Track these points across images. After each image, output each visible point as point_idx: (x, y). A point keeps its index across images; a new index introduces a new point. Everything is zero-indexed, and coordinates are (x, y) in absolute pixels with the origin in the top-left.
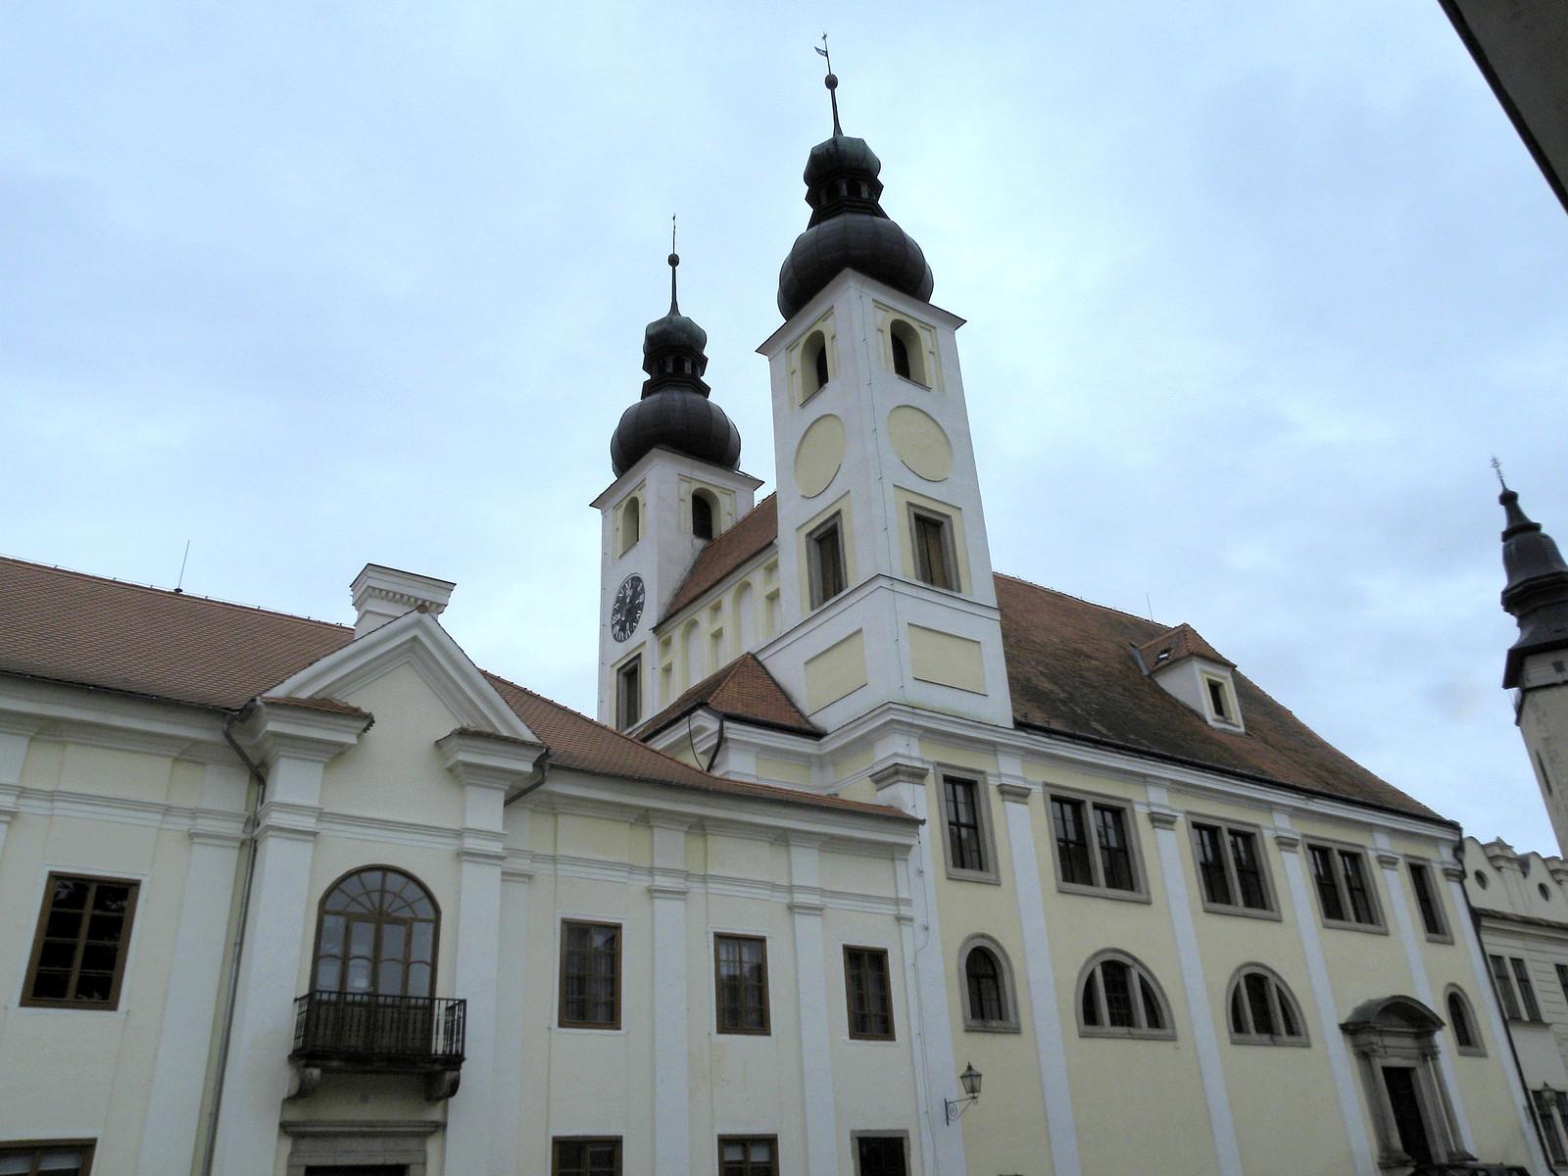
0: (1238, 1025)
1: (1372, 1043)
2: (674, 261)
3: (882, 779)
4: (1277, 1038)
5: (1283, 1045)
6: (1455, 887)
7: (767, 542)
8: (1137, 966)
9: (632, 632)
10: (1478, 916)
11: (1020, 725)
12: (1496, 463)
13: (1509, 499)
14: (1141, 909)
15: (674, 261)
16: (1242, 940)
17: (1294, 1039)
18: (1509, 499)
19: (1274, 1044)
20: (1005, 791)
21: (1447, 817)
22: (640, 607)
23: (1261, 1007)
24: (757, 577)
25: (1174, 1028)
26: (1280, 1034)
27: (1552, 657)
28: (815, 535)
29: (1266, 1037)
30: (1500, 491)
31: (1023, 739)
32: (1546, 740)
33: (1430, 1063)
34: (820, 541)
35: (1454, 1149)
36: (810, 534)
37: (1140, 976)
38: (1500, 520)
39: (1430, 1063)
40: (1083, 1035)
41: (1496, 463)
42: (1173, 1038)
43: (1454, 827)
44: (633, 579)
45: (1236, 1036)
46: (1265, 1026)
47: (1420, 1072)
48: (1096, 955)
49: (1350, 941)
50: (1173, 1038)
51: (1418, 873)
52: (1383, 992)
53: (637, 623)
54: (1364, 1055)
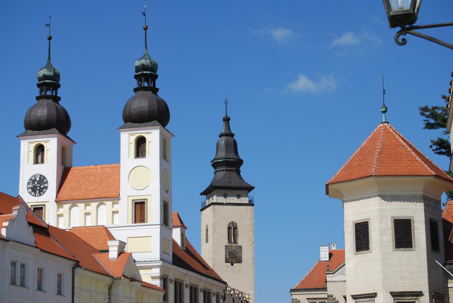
3: (153, 278)
6: (222, 300)
7: (114, 194)
9: (40, 195)
11: (174, 264)
12: (226, 102)
13: (227, 120)
15: (50, 39)
18: (227, 120)
20: (170, 280)
21: (224, 280)
22: (46, 188)
24: (109, 204)
28: (136, 201)
30: (224, 115)
32: (214, 224)
34: (136, 203)
36: (133, 200)
41: (226, 102)
43: (225, 283)
44: (41, 175)
51: (218, 296)
53: (44, 193)
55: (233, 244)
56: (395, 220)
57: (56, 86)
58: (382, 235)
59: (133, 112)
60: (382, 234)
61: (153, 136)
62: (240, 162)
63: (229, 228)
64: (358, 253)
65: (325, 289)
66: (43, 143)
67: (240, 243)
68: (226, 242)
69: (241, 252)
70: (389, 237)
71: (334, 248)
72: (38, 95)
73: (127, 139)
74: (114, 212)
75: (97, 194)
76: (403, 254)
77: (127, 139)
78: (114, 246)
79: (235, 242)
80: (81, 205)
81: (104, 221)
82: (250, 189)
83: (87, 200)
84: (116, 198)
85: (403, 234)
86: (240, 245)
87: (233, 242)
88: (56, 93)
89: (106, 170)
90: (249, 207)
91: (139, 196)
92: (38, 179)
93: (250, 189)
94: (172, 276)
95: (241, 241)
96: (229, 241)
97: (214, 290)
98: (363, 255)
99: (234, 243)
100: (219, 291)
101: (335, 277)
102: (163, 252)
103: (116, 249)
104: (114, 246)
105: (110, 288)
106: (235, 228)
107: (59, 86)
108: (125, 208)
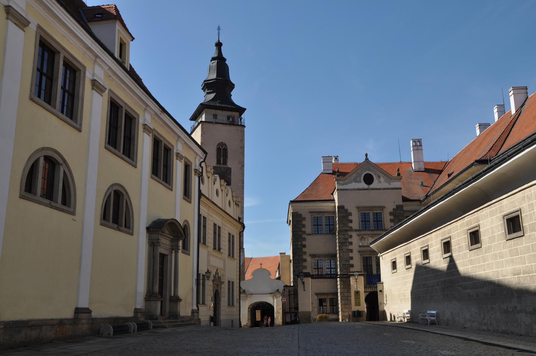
0: (105, 216)
1: (159, 239)
4: (120, 228)
5: (122, 231)
8: (64, 165)
10: (200, 194)
12: (219, 29)
13: (219, 45)
14: (76, 132)
16: (118, 170)
17: (127, 230)
18: (219, 45)
19: (119, 230)
23: (116, 210)
25: (75, 208)
26: (122, 226)
27: (214, 111)
29: (116, 226)
30: (217, 41)
33: (173, 255)
35: (172, 295)
37: (64, 172)
38: (213, 53)
39: (173, 255)
40: (22, 197)
41: (219, 29)
42: (73, 213)
45: (103, 222)
46: (116, 220)
47: (169, 256)
48: (43, 149)
49: (160, 188)
50: (73, 213)
51: (187, 167)
52: (166, 216)
54: (153, 244)
55: (222, 166)
62: (232, 86)
63: (218, 150)
67: (229, 164)
69: (230, 174)
79: (225, 163)
82: (241, 110)
86: (229, 166)
87: (222, 162)
90: (240, 128)
93: (241, 110)
96: (218, 162)
99: (223, 164)
100: (191, 157)
101: (347, 184)
106: (225, 150)
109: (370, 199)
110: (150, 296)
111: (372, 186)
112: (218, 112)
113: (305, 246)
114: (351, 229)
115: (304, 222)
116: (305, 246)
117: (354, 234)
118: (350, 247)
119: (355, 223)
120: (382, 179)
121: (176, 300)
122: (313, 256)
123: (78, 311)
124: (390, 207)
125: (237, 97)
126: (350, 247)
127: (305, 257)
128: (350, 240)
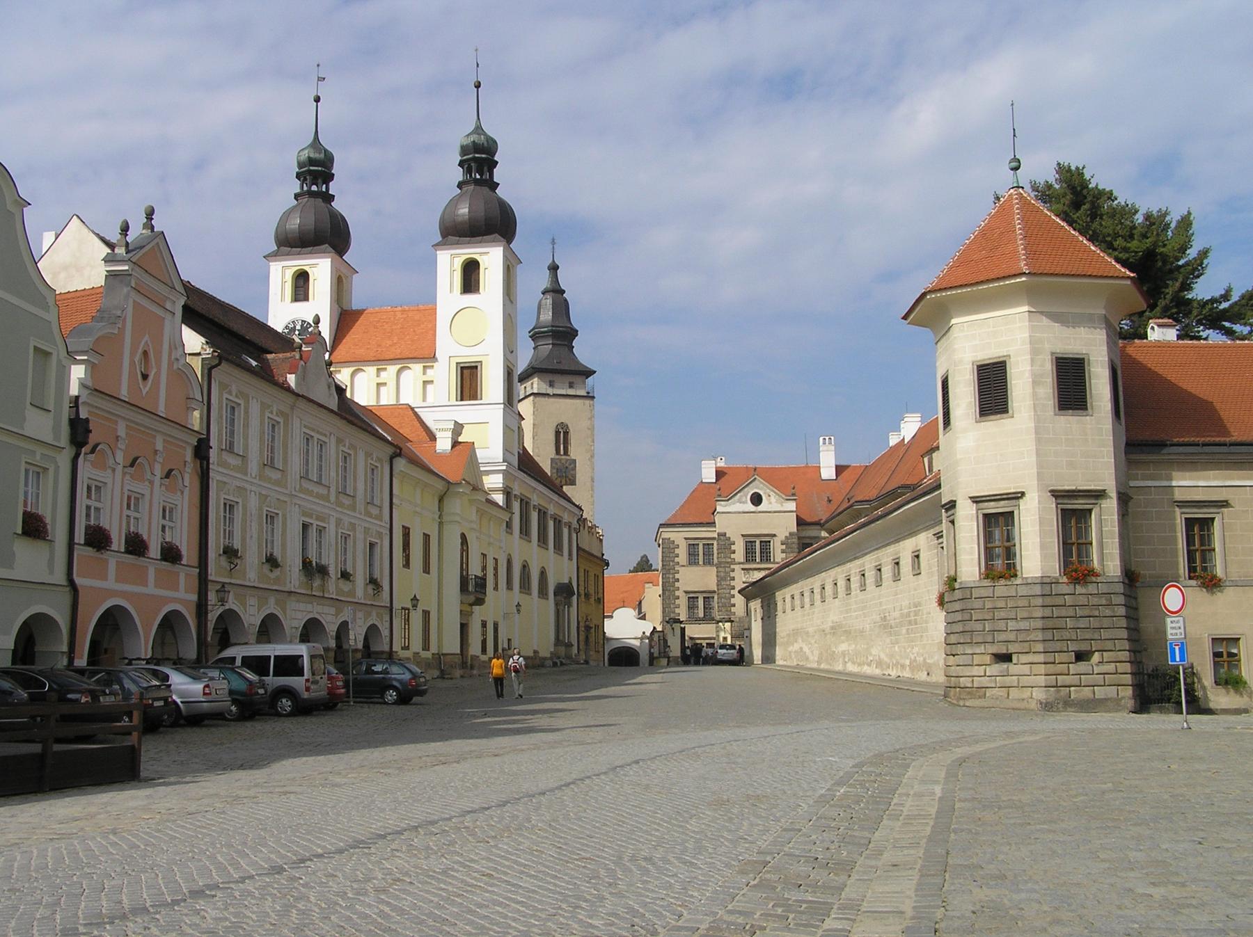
2: (317, 100)
12: (553, 242)
13: (554, 268)
24: (417, 368)
27: (550, 377)
31: (521, 475)
38: (544, 281)
41: (553, 242)
54: (557, 604)
56: (1057, 359)
57: (328, 177)
58: (1029, 386)
59: (460, 219)
60: (1035, 383)
61: (491, 258)
62: (574, 333)
63: (557, 433)
64: (984, 418)
65: (713, 524)
66: (306, 268)
68: (552, 453)
70: (1048, 390)
71: (721, 464)
72: (298, 190)
73: (449, 262)
74: (425, 383)
75: (397, 352)
76: (1071, 421)
77: (449, 262)
78: (446, 430)
79: (566, 453)
80: (371, 370)
81: (410, 397)
82: (589, 373)
83: (380, 361)
84: (428, 357)
85: (1070, 384)
88: (327, 188)
89: (410, 314)
90: (588, 402)
91: (469, 356)
92: (298, 327)
93: (589, 373)
94: (517, 490)
95: (574, 452)
96: (558, 452)
97: (566, 518)
98: (995, 426)
102: (506, 450)
103: (449, 434)
104: (446, 430)
105: (441, 500)
106: (566, 433)
107: (331, 177)
108: (444, 376)
109: (759, 526)
110: (558, 641)
111: (760, 508)
112: (556, 378)
113: (678, 580)
114: (733, 562)
115: (677, 551)
116: (678, 580)
117: (736, 567)
118: (733, 583)
119: (739, 555)
120: (773, 499)
121: (570, 645)
122: (686, 592)
123: (535, 652)
124: (782, 534)
125: (583, 350)
126: (733, 583)
127: (677, 593)
128: (732, 574)
